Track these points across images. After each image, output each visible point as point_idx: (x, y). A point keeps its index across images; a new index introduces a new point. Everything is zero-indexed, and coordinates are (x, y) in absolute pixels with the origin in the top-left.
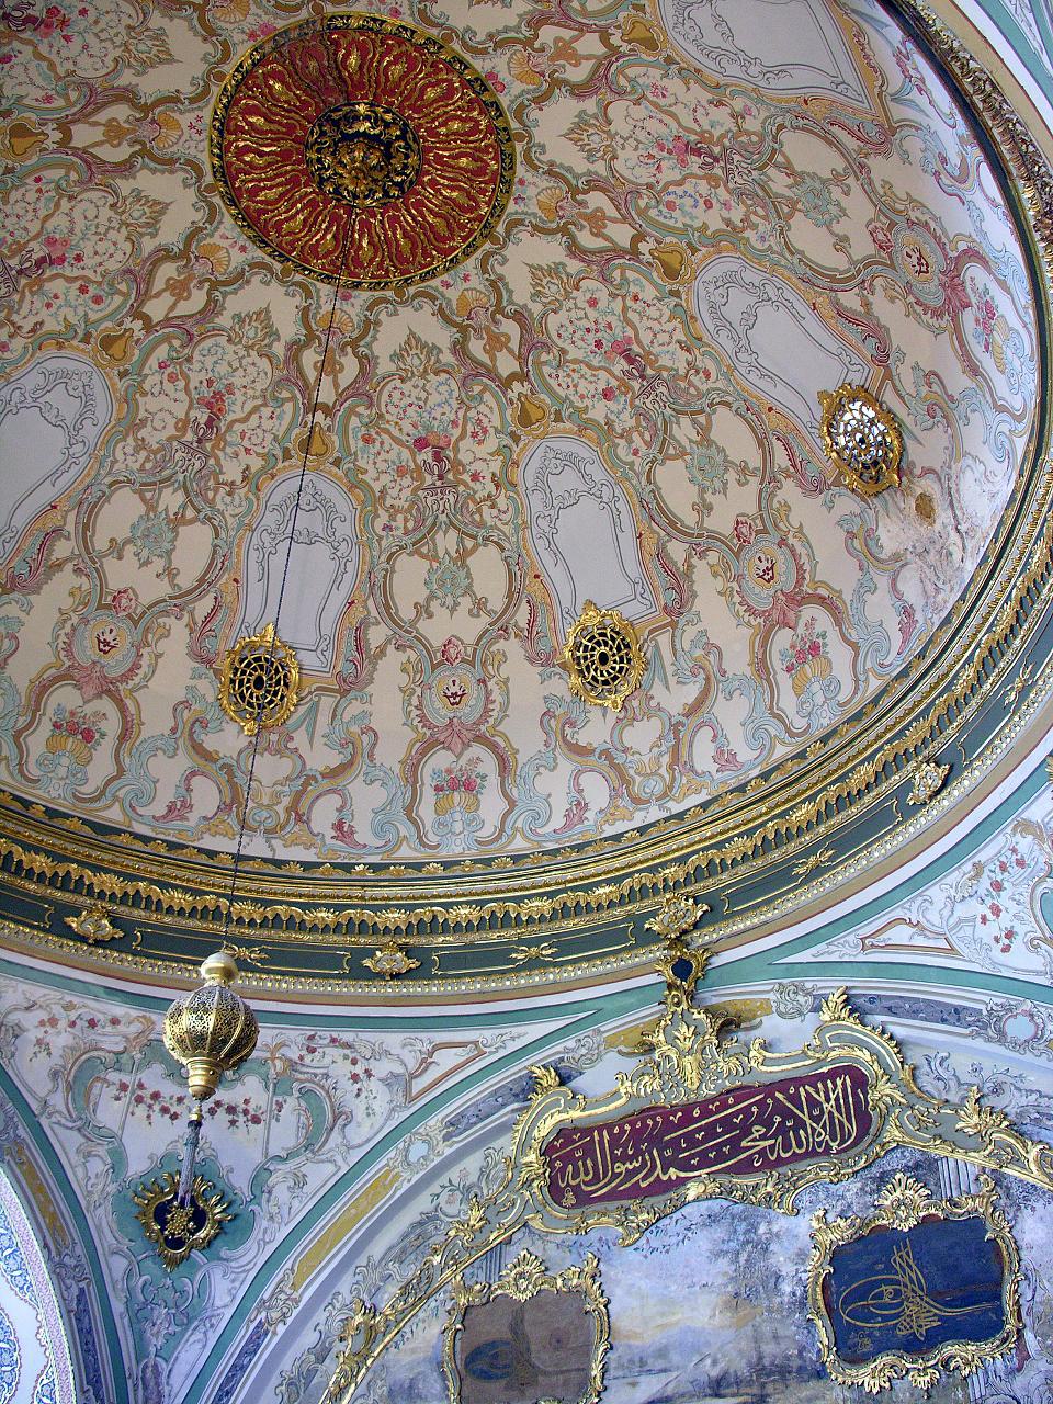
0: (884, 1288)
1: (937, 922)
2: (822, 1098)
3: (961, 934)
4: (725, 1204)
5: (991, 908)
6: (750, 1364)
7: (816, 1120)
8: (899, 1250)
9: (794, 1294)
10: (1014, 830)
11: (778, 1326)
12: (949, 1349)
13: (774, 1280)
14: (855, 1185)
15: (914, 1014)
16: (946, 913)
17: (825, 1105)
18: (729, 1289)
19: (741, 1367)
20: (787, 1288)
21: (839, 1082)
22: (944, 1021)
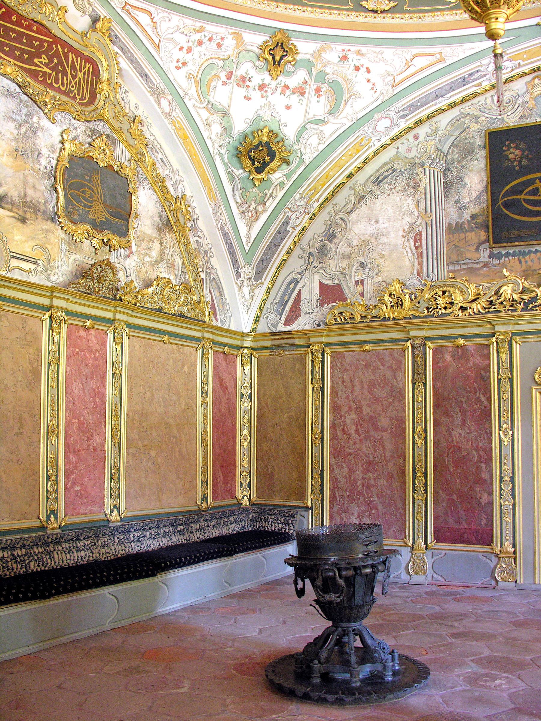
0: (87, 189)
1: (163, 31)
2: (78, 67)
3: (167, 44)
4: (18, 90)
5: (189, 47)
6: (19, 195)
7: (74, 77)
8: (96, 175)
9: (46, 168)
10: (232, 33)
11: (36, 181)
12: (111, 237)
13: (37, 154)
14: (83, 128)
15: (132, 62)
16: (171, 31)
17: (79, 72)
18: (13, 144)
19: (14, 194)
20: (43, 162)
21: (88, 66)
22: (141, 76)
